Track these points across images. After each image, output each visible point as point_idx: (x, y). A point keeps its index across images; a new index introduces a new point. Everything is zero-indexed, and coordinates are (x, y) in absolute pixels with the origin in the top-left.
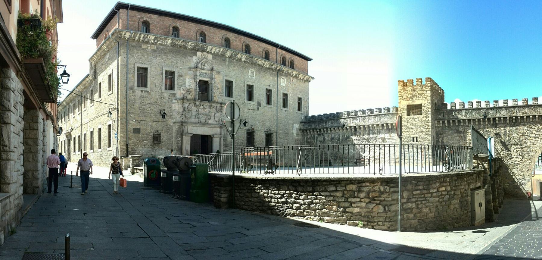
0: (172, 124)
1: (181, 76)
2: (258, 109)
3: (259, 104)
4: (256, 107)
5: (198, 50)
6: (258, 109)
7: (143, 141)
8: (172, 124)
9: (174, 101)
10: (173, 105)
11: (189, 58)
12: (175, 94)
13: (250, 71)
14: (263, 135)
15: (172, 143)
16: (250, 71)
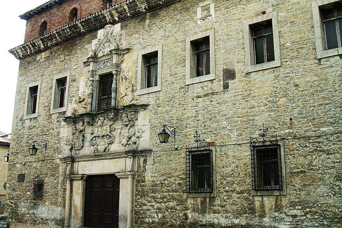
0: (58, 161)
1: (75, 81)
2: (226, 87)
3: (229, 74)
4: (218, 86)
5: (97, 29)
6: (226, 87)
7: (26, 192)
8: (58, 161)
9: (63, 123)
10: (62, 130)
11: (86, 46)
12: (64, 112)
13: (199, 10)
14: (246, 154)
15: (57, 195)
16: (199, 10)
